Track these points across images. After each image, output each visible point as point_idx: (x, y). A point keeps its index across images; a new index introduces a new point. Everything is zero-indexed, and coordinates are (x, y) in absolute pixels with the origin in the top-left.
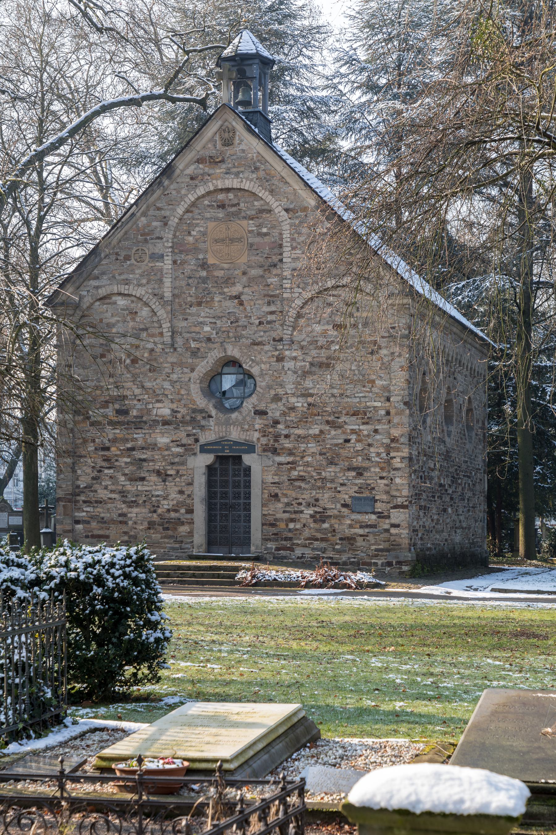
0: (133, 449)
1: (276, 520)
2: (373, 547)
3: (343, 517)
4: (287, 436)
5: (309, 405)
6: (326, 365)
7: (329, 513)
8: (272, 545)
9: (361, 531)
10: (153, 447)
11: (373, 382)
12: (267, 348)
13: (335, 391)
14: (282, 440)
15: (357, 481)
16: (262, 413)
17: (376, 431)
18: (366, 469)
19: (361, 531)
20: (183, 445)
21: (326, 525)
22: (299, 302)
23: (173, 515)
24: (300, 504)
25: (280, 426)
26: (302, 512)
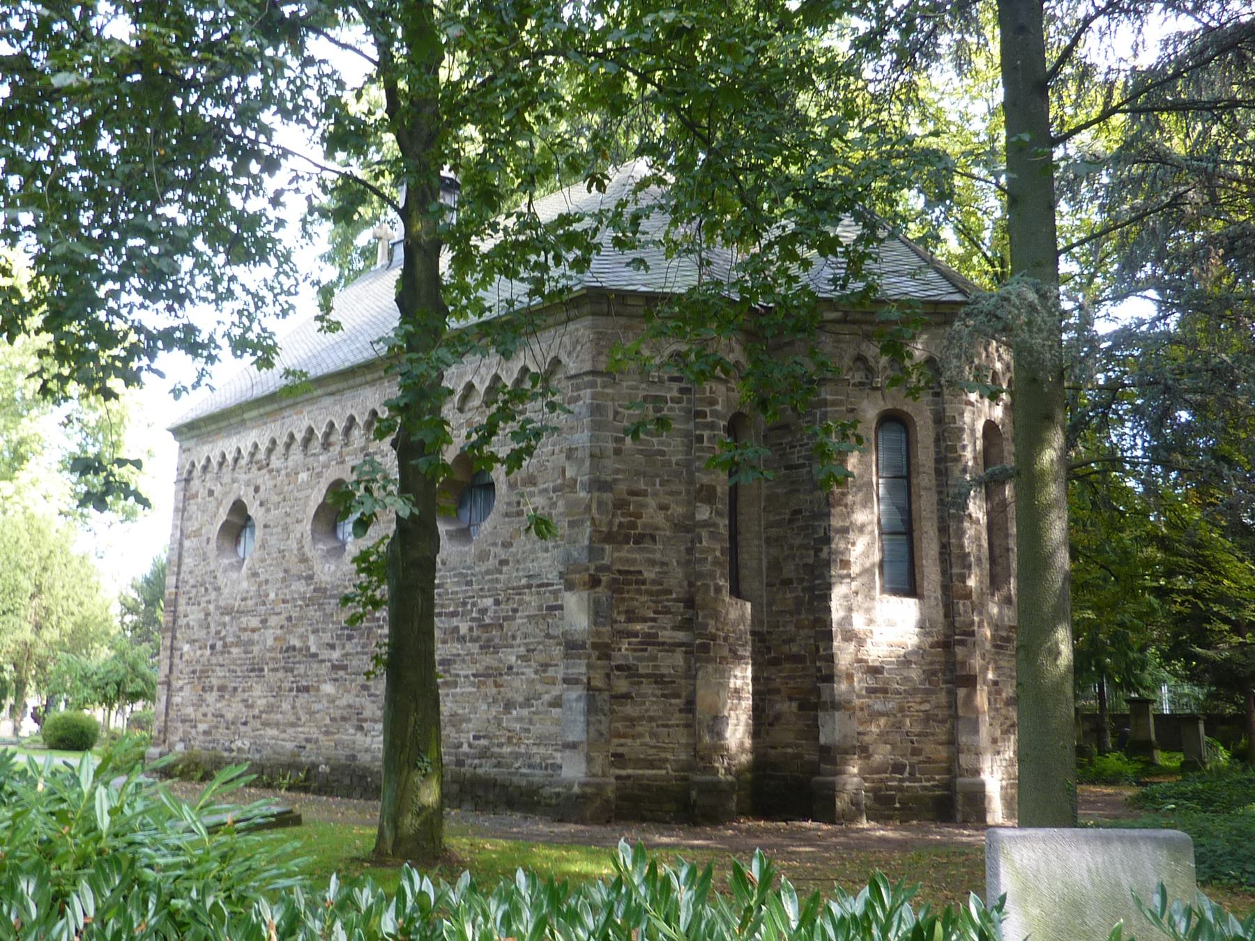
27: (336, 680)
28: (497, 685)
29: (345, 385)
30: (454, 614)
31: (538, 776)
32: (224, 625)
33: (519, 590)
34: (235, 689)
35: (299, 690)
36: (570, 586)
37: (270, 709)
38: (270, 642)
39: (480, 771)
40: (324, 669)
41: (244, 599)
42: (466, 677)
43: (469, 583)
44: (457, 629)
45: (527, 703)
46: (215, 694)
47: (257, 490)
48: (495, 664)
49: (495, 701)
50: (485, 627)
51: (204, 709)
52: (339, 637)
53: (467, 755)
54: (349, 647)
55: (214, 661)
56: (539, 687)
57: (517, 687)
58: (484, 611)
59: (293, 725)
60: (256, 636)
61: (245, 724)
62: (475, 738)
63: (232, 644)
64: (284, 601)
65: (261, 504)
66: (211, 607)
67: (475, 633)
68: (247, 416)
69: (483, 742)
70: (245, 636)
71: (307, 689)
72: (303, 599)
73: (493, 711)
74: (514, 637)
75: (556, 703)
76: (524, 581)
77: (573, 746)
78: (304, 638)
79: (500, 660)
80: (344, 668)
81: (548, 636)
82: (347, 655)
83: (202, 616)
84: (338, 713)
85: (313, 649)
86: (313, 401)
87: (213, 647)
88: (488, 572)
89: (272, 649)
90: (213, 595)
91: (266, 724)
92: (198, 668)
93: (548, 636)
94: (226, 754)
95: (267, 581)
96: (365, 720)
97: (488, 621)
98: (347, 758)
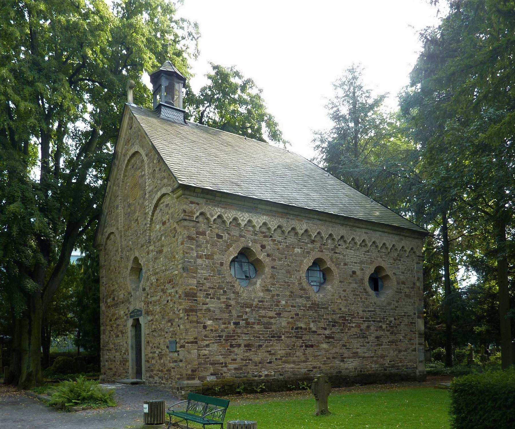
0: (116, 319)
1: (149, 358)
2: (177, 376)
3: (167, 355)
5: (157, 280)
12: (145, 247)
13: (164, 268)
14: (150, 306)
15: (171, 329)
19: (172, 365)
20: (126, 315)
21: (162, 361)
22: (150, 213)
23: (125, 356)
25: (149, 296)
26: (155, 352)
27: (328, 342)
28: (396, 345)
29: (330, 220)
30: (380, 322)
31: (410, 371)
32: (246, 313)
33: (402, 316)
34: (260, 346)
35: (307, 346)
36: (419, 317)
37: (288, 355)
38: (284, 324)
39: (392, 371)
40: (321, 338)
41: (262, 301)
42: (386, 342)
43: (385, 312)
44: (381, 327)
45: (406, 351)
46: (243, 347)
47: (263, 247)
48: (395, 339)
49: (396, 350)
50: (392, 327)
51: (233, 356)
52: (328, 325)
53: (387, 367)
54: (334, 329)
55: (239, 331)
56: (409, 346)
57: (402, 346)
58: (391, 322)
59: (304, 362)
60: (272, 321)
61: (270, 363)
62: (390, 361)
63: (254, 323)
64: (292, 306)
65: (268, 255)
66: (232, 302)
67: (388, 328)
68: (259, 206)
69: (392, 363)
70: (265, 320)
71: (312, 346)
72: (305, 306)
73: (395, 353)
74: (401, 331)
75: (415, 350)
76: (403, 314)
77: (421, 362)
79: (397, 337)
80: (333, 338)
81: (411, 331)
82: (333, 332)
83: (223, 306)
84: (331, 356)
85: (314, 329)
86: (309, 219)
87: (236, 324)
88: (392, 309)
89: (285, 328)
90: (232, 296)
91: (286, 362)
92: (224, 334)
93: (411, 331)
94: (256, 378)
95: (278, 295)
96: (345, 358)
97: (392, 325)
98: (337, 373)
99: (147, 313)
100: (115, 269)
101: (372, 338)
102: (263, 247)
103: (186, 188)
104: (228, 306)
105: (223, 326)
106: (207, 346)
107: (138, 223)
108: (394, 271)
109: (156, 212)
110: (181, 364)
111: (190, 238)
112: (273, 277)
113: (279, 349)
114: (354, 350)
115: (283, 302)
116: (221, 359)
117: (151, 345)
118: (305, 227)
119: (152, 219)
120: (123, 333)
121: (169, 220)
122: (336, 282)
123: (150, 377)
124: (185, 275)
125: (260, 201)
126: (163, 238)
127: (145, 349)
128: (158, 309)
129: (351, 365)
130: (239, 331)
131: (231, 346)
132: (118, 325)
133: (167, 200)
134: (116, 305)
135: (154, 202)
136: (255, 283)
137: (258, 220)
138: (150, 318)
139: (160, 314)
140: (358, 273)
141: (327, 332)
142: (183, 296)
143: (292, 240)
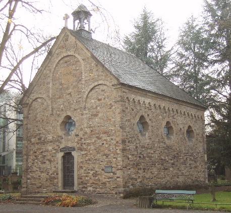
0: (42, 152)
1: (82, 176)
4: (84, 144)
6: (96, 115)
7: (98, 173)
8: (81, 186)
9: (108, 180)
10: (47, 151)
11: (110, 120)
16: (77, 135)
17: (112, 139)
18: (109, 155)
19: (108, 180)
20: (55, 150)
21: (97, 178)
22: (87, 93)
23: (53, 176)
24: (89, 170)
25: (83, 140)
26: (89, 173)
32: (143, 151)
37: (158, 174)
47: (148, 115)
59: (165, 178)
66: (138, 145)
68: (148, 94)
71: (167, 169)
78: (165, 157)
87: (140, 157)
90: (138, 142)
99: (81, 150)
100: (43, 121)
101: (188, 165)
102: (148, 115)
103: (123, 84)
104: (137, 147)
105: (135, 158)
106: (129, 169)
107: (71, 96)
108: (195, 128)
109: (91, 93)
110: (118, 179)
111: (123, 111)
112: (152, 131)
113: (155, 171)
114: (182, 172)
115: (156, 145)
116: (134, 176)
117: (84, 168)
118: (163, 105)
119: (87, 96)
120: (50, 161)
121: (105, 99)
122: (174, 134)
123: (82, 188)
124: (121, 130)
125: (149, 92)
126: (99, 108)
127: (78, 171)
128: (92, 147)
129: (181, 179)
130: (140, 161)
131: (138, 169)
132: (45, 156)
133: (102, 87)
134: (44, 143)
135: (92, 87)
136: (145, 135)
137: (147, 101)
138: (83, 153)
139: (95, 151)
140: (182, 129)
141: (172, 161)
142: (120, 142)
143: (158, 111)
